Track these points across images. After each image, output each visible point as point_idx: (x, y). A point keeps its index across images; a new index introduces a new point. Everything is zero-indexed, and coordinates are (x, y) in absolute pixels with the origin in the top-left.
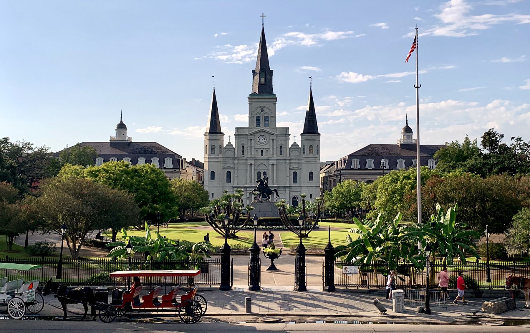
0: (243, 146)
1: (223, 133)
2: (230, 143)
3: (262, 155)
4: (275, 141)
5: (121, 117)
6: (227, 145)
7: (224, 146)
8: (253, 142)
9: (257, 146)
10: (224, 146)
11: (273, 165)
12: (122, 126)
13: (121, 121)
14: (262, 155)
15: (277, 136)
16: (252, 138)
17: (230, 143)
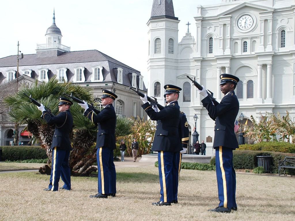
0: (211, 38)
1: (177, 19)
2: (188, 34)
3: (245, 50)
4: (270, 24)
5: (54, 18)
6: (184, 39)
7: (179, 41)
8: (228, 28)
9: (236, 35)
10: (179, 41)
11: (264, 66)
12: (56, 31)
13: (54, 23)
14: (245, 50)
15: (275, 12)
16: (227, 21)
17: (188, 34)
